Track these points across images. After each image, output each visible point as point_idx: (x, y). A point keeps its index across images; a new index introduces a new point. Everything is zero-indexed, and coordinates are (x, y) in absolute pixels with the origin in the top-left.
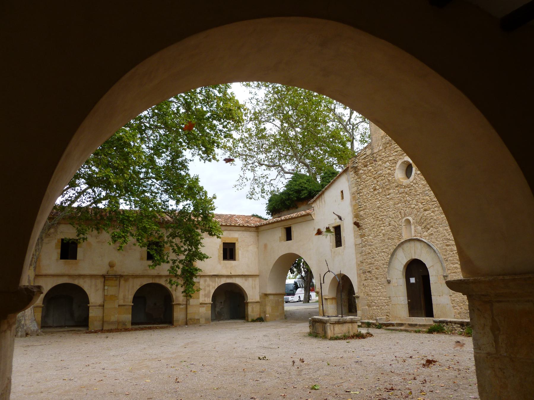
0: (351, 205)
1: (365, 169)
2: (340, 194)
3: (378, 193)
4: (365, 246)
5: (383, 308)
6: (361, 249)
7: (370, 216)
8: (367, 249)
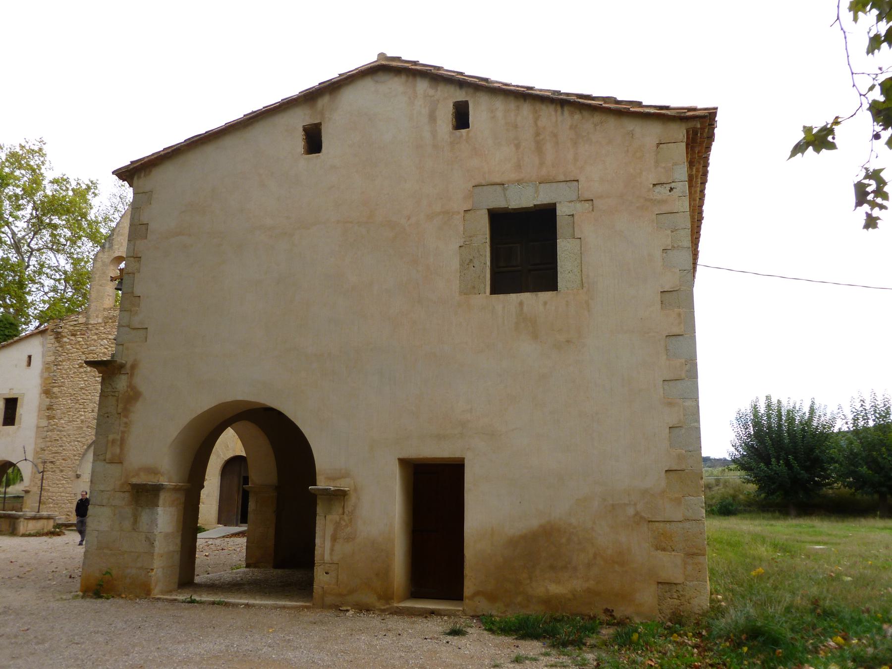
0: (41, 377)
1: (73, 338)
2: (26, 359)
4: (51, 431)
6: (45, 433)
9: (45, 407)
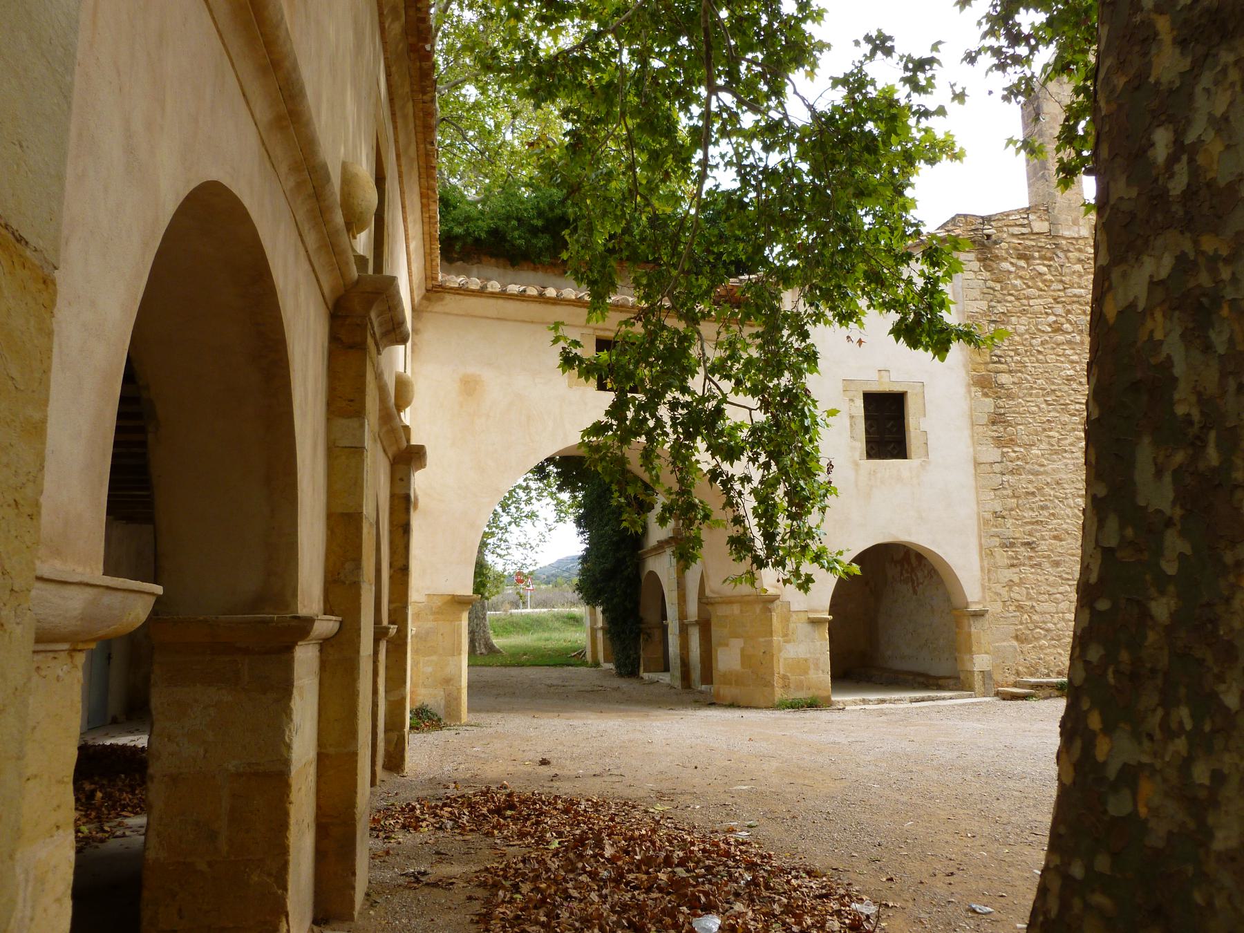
1: (1022, 263)
3: (1069, 342)
6: (999, 479)
7: (1037, 396)
8: (1022, 482)
9: (985, 421)
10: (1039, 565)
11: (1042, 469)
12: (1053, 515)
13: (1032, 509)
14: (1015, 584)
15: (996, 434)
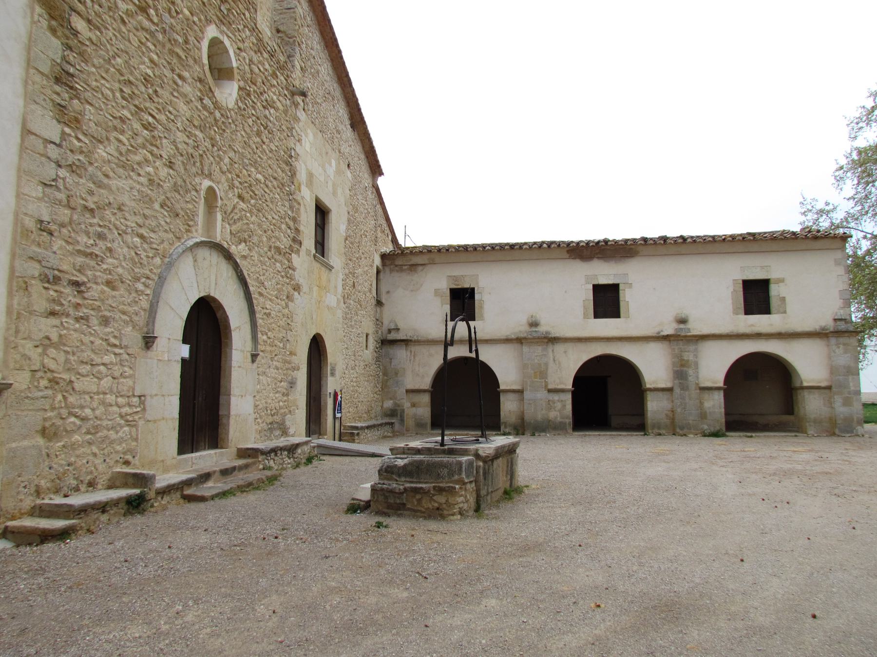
5: (112, 434)
10: (85, 319)
11: (106, 181)
12: (110, 250)
13: (87, 234)
14: (52, 345)
15: (58, 100)
